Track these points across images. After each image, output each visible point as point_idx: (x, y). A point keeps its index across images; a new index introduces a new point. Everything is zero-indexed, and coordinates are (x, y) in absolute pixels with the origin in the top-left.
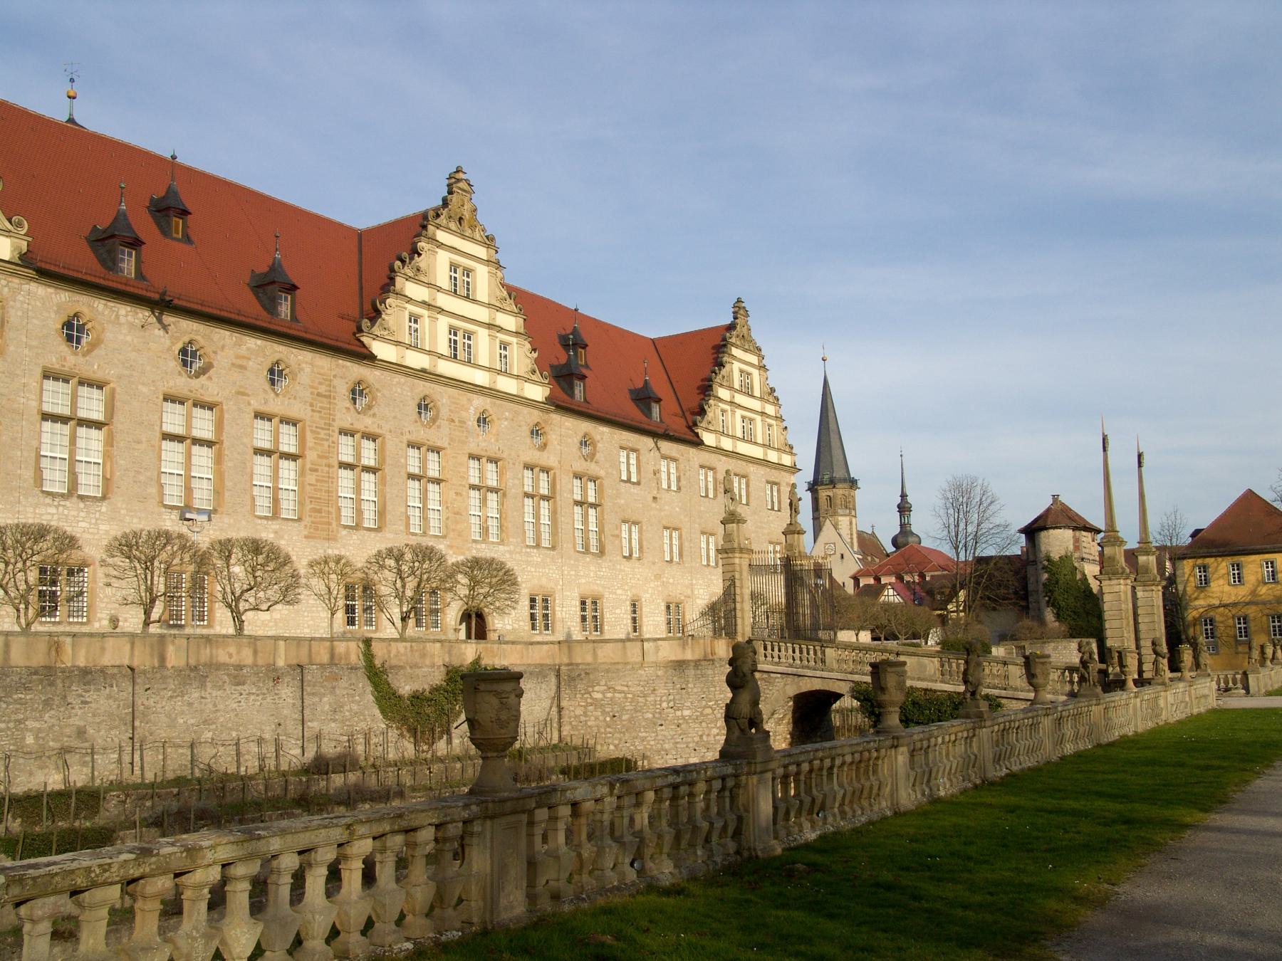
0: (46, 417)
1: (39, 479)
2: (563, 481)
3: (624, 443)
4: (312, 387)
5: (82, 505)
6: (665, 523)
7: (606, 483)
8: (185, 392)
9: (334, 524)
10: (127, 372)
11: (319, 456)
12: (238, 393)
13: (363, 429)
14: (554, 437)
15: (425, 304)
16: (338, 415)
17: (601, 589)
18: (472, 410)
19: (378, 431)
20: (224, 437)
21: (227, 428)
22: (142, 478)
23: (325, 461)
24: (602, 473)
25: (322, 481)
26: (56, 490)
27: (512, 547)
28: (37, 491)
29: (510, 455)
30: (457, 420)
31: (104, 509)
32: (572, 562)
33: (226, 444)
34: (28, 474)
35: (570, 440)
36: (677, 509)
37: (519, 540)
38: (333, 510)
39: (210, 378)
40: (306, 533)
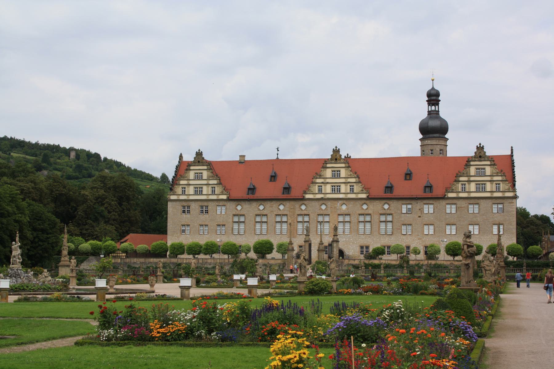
0: (234, 222)
1: (232, 233)
3: (403, 203)
6: (425, 223)
7: (394, 215)
8: (260, 214)
9: (295, 234)
12: (271, 212)
13: (303, 214)
15: (322, 183)
17: (391, 244)
18: (339, 204)
19: (307, 213)
21: (268, 219)
23: (293, 222)
24: (393, 212)
30: (333, 207)
33: (268, 221)
34: (231, 232)
37: (356, 233)
38: (295, 232)
40: (288, 236)
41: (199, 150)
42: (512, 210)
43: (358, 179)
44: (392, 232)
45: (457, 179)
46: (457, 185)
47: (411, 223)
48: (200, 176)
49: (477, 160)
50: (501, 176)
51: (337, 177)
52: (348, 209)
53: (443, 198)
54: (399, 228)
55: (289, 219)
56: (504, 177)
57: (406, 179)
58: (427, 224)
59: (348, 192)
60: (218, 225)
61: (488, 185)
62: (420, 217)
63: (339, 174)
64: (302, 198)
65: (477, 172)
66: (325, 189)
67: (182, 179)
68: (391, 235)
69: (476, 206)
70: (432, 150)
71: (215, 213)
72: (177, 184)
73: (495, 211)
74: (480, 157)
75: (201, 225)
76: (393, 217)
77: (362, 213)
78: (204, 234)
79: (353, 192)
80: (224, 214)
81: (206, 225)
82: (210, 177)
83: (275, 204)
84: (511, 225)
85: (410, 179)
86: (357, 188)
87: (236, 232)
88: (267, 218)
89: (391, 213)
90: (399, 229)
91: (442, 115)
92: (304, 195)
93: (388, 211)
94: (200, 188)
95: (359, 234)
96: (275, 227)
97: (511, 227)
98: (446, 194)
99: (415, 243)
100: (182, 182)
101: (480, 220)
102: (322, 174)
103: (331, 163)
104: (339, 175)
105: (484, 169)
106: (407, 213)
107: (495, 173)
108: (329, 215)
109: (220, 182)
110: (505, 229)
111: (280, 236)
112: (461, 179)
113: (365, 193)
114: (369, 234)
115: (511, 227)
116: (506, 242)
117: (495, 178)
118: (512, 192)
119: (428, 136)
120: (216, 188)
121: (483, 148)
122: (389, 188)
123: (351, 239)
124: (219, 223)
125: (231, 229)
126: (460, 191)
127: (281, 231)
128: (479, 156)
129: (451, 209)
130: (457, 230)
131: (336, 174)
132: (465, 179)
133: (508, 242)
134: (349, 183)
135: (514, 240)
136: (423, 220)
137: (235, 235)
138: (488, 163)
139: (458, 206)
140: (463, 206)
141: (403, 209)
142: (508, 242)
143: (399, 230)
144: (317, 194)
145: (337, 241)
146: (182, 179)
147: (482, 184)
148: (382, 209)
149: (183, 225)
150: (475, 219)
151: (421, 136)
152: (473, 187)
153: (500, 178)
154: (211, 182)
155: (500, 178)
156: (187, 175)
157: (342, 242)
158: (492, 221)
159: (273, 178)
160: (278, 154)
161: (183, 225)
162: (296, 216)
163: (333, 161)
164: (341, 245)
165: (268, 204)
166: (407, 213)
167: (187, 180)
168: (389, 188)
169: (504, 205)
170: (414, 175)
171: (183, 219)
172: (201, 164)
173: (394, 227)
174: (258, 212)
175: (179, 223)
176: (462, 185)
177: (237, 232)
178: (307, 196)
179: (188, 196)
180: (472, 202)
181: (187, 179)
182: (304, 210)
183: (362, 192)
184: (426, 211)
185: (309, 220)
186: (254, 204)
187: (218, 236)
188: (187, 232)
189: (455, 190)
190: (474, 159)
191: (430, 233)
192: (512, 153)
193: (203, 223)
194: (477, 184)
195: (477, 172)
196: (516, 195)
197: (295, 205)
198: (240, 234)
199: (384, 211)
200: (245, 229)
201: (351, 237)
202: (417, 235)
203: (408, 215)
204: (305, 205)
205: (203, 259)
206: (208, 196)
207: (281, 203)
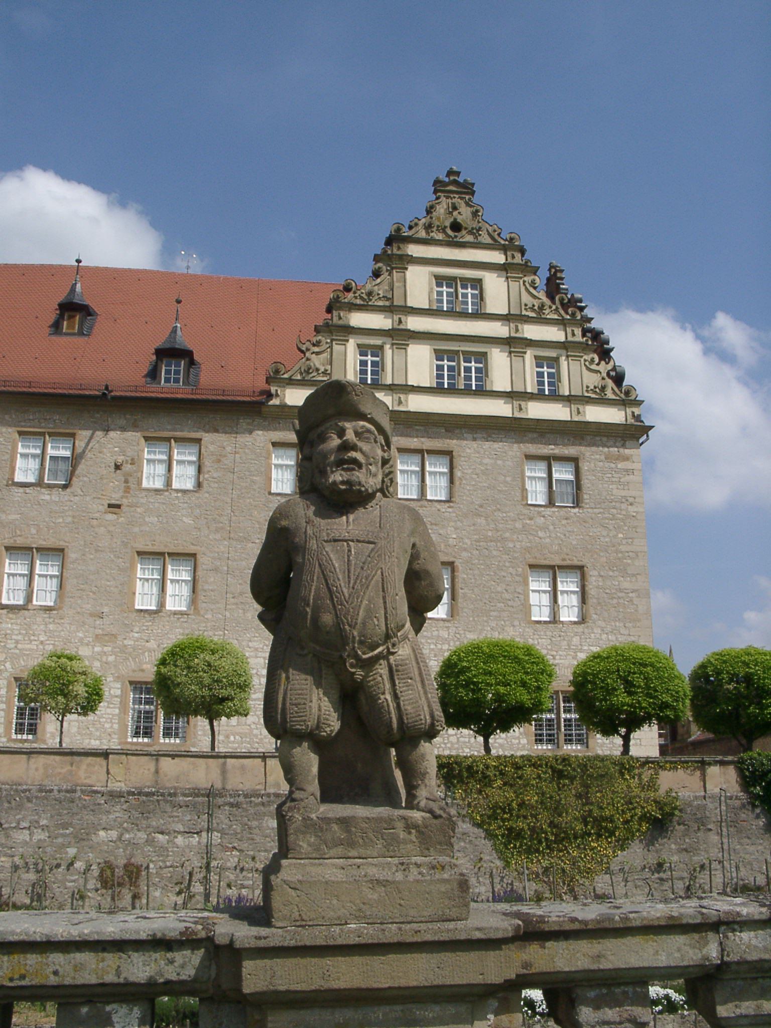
42: (624, 493)
46: (337, 348)
62: (118, 506)
65: (440, 294)
69: (436, 468)
73: (537, 494)
110: (591, 590)
115: (626, 585)
136: (136, 530)
138: (498, 257)
141: (20, 462)
158: (528, 550)
166: (40, 483)
169: (584, 467)
196: (638, 418)
202: (91, 615)
203: (46, 495)
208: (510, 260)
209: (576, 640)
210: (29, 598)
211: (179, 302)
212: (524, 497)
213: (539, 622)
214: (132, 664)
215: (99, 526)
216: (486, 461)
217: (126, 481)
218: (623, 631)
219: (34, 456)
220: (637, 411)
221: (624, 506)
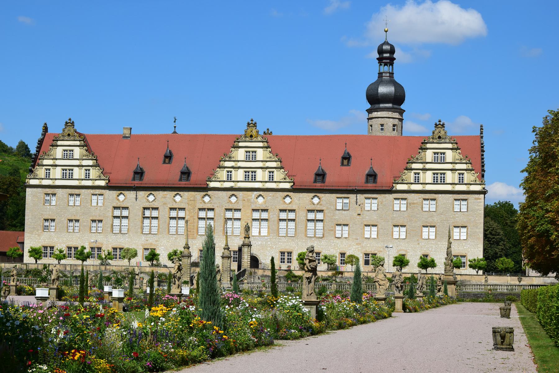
2: (300, 214)
4: (188, 199)
5: (121, 235)
7: (326, 211)
8: (148, 206)
9: (195, 235)
10: (133, 204)
11: (191, 217)
14: (295, 199)
15: (233, 167)
16: (198, 205)
17: (321, 250)
18: (253, 196)
20: (160, 216)
22: (136, 228)
23: (192, 218)
25: (191, 223)
26: (117, 232)
27: (271, 237)
28: (111, 233)
29: (271, 207)
30: (246, 200)
31: (127, 236)
32: (304, 240)
34: (109, 229)
35: (305, 199)
36: (375, 217)
38: (195, 231)
39: (155, 202)
41: (70, 120)
42: (479, 208)
43: (279, 163)
44: (323, 235)
45: (409, 166)
46: (409, 174)
47: (348, 223)
48: (70, 154)
49: (435, 141)
50: (466, 163)
51: (253, 159)
52: (265, 202)
53: (390, 191)
54: (332, 229)
55: (187, 214)
56: (470, 165)
57: (342, 164)
58: (369, 224)
59: (266, 180)
60: (94, 221)
61: (449, 174)
62: (360, 214)
63: (255, 155)
64: (205, 186)
66: (236, 176)
67: (46, 157)
68: (321, 238)
70: (382, 125)
71: (89, 204)
72: (39, 165)
74: (439, 137)
75: (71, 220)
76: (324, 215)
77: (284, 208)
78: (74, 232)
79: (272, 180)
80: (101, 206)
81: (77, 221)
82: (84, 156)
83: (169, 194)
84: (477, 227)
85: (348, 165)
86: (278, 175)
87: (116, 230)
88: (159, 212)
89: (322, 209)
90: (332, 230)
91: (396, 78)
92: (208, 183)
93: (318, 206)
94: (70, 171)
95: (279, 236)
96: (169, 224)
97: (477, 231)
98: (394, 185)
99: (353, 249)
100: (45, 162)
101: (437, 220)
102: (233, 155)
103: (245, 141)
104: (255, 157)
105: (444, 153)
106: (342, 210)
107: (458, 160)
108: (240, 210)
109: (97, 162)
111: (175, 236)
112: (414, 166)
113: (289, 182)
114: (293, 237)
115: (477, 231)
116: (470, 250)
117: (458, 166)
118: (480, 184)
119: (377, 106)
120: (91, 170)
121: (443, 126)
122: (321, 175)
123: (269, 243)
124: (94, 219)
125: (110, 226)
126: (412, 182)
127: (177, 230)
128: (437, 137)
129: (400, 206)
130: (407, 232)
131: (251, 157)
132: (420, 166)
133: (472, 249)
134: (267, 168)
135: (480, 247)
136: (364, 220)
137: (115, 234)
138: (450, 146)
139: (409, 201)
140: (415, 202)
142: (472, 249)
143: (332, 232)
144: (224, 181)
145: (249, 245)
146: (46, 157)
147: (441, 174)
148: (311, 204)
149: (46, 220)
150: (430, 220)
151: (369, 106)
152: (428, 177)
153: (464, 166)
154: (85, 163)
155: (464, 166)
156: (52, 152)
157: (257, 246)
158: (453, 223)
159: (168, 158)
160: (175, 127)
161: (46, 220)
162: (196, 211)
163: (247, 139)
164: (255, 251)
165: (160, 194)
166: (342, 210)
167: (52, 159)
168: (321, 175)
169: (469, 201)
170: (353, 160)
171: (45, 212)
172: (72, 138)
173: (325, 228)
174: (147, 205)
175: (41, 217)
176: (415, 174)
177: (119, 230)
178: (212, 185)
179: (53, 181)
180: (427, 197)
181: (52, 158)
182: (207, 203)
183: (285, 181)
184: (367, 207)
185: (214, 216)
186: (141, 194)
187: (93, 234)
188: (53, 229)
189: (406, 180)
190: (431, 140)
191: (373, 237)
192: (482, 133)
193: (73, 218)
194: (434, 174)
195: (435, 157)
196: (484, 188)
197: (196, 196)
198: (121, 233)
199: (313, 206)
200: (129, 226)
201: (269, 240)
202: (355, 239)
203: (343, 212)
204: (209, 196)
205: (71, 265)
206: (80, 181)
207: (176, 192)
208: (453, 147)
209: (464, 244)
210: (342, 236)
211: (371, 160)
212: (453, 210)
213: (455, 240)
214: (364, 250)
215: (356, 219)
216: (444, 201)
217: (361, 209)
218: (475, 242)
219: (341, 203)
220: (483, 186)
221: (478, 211)
